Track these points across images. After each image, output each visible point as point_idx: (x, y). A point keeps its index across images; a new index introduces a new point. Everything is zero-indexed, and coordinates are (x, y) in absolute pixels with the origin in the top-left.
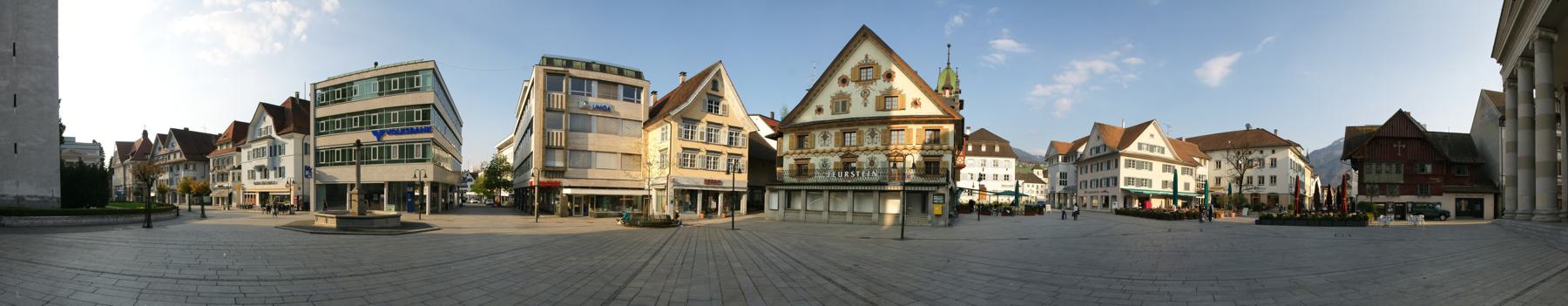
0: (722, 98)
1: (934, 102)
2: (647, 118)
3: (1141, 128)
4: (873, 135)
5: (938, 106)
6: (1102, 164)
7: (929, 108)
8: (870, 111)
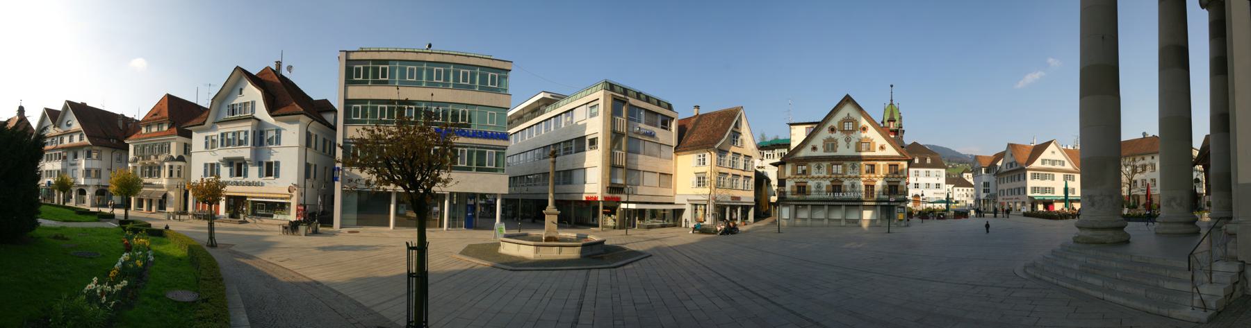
0: (740, 133)
1: (894, 147)
2: (677, 144)
3: (1044, 147)
5: (897, 150)
7: (891, 151)
8: (851, 152)
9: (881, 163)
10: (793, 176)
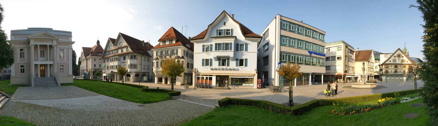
4: (400, 66)
5: (411, 62)
8: (400, 62)
9: (407, 65)
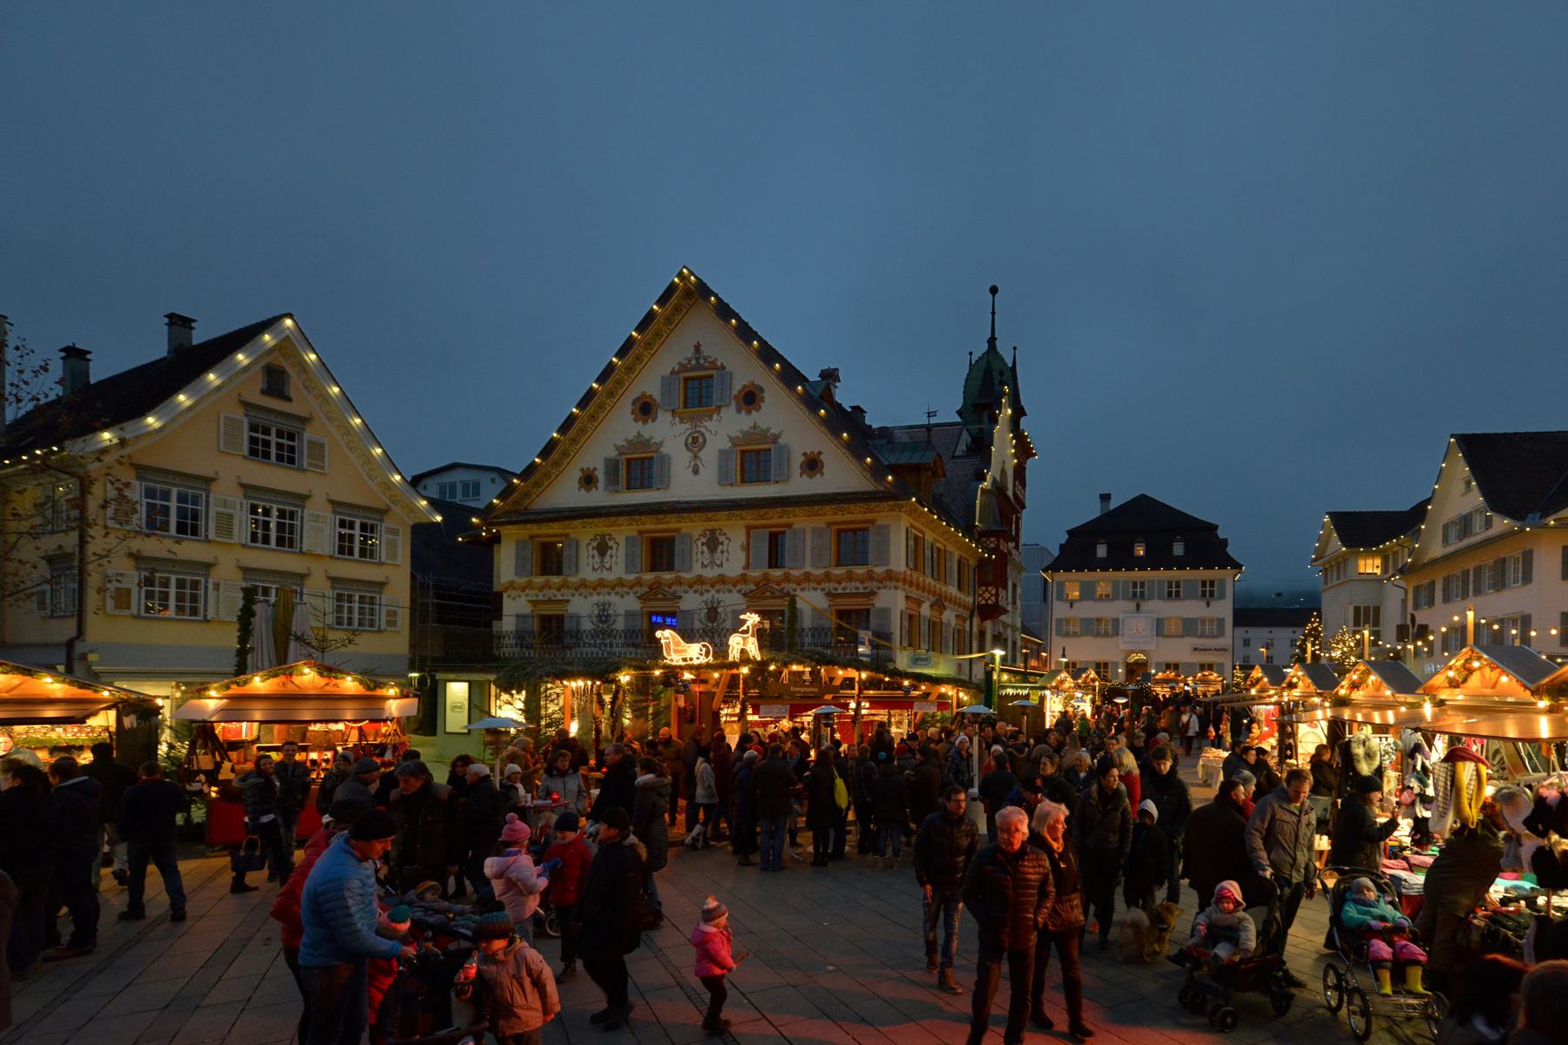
6: (1478, 570)
10: (522, 581)
